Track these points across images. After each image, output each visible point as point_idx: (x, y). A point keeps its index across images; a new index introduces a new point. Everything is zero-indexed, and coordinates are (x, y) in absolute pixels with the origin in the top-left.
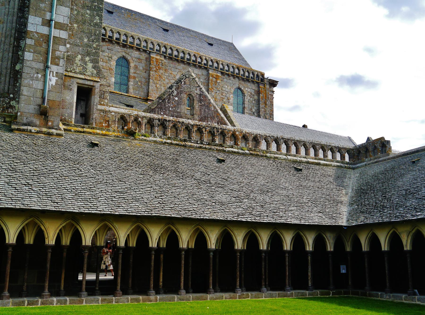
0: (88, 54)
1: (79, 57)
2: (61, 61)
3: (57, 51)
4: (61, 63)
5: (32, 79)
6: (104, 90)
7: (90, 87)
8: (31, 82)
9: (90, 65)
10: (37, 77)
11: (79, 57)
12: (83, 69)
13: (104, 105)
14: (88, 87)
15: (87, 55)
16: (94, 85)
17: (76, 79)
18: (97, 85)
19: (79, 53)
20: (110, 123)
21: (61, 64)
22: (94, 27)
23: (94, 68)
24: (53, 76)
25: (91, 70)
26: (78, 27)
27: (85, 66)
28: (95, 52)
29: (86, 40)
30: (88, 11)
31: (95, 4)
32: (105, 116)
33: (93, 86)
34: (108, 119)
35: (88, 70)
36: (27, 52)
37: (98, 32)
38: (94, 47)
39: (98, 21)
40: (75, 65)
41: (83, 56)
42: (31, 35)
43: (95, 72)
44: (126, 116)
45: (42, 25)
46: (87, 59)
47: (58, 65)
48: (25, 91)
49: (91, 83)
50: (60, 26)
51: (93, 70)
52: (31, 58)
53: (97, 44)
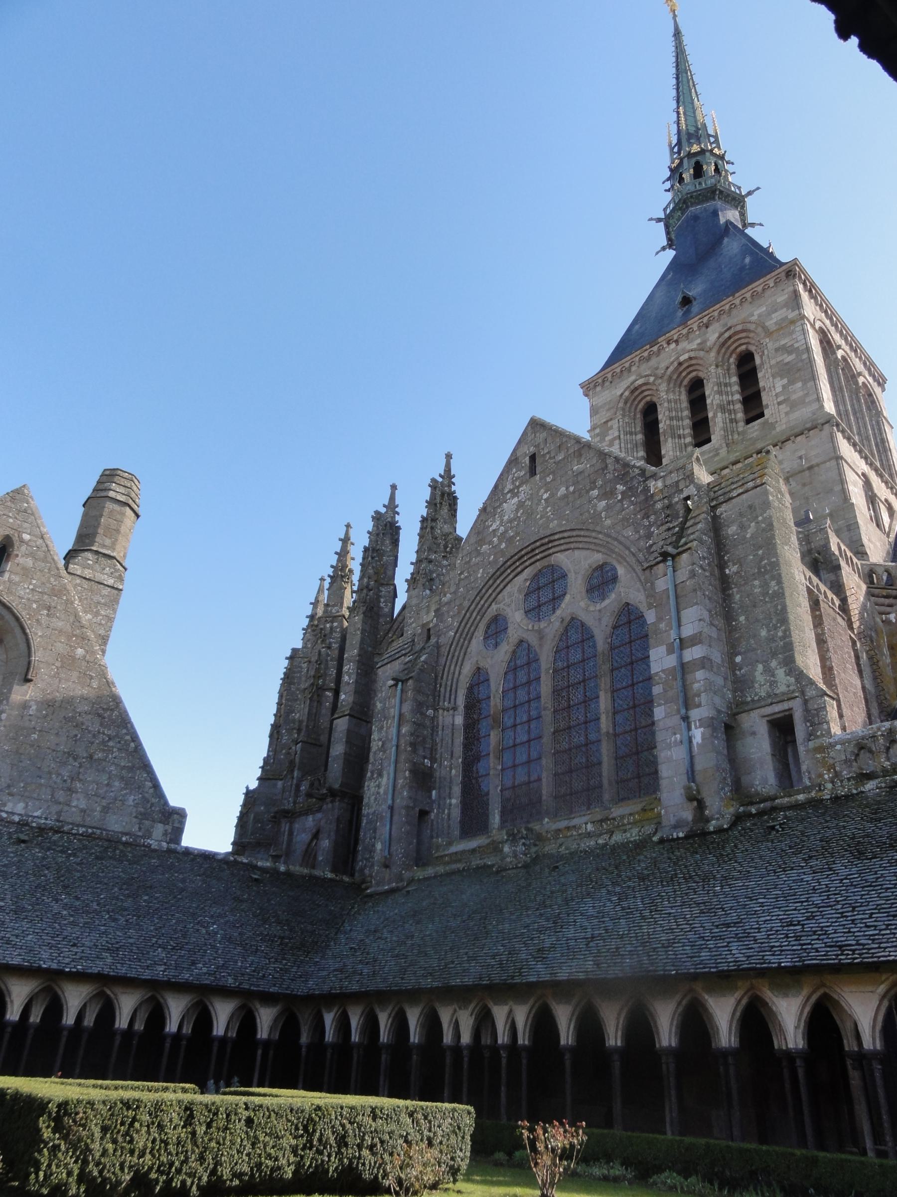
0: (774, 654)
1: (760, 667)
2: (703, 695)
3: (694, 683)
4: (702, 700)
5: (669, 746)
6: (816, 706)
7: (787, 713)
8: (669, 753)
9: (780, 673)
10: (676, 740)
11: (760, 667)
12: (771, 685)
13: (822, 735)
14: (785, 715)
15: (773, 657)
16: (791, 706)
17: (758, 711)
18: (796, 705)
19: (757, 661)
20: (838, 769)
21: (703, 703)
22: (771, 602)
23: (789, 675)
24: (696, 728)
25: (785, 682)
26: (747, 619)
27: (772, 679)
28: (784, 643)
29: (764, 633)
30: (756, 583)
31: (763, 563)
32: (824, 758)
33: (791, 709)
34: (831, 761)
35: (779, 684)
36: (658, 706)
37: (779, 607)
38: (780, 638)
39: (776, 588)
40: (756, 685)
41: (766, 663)
42: (657, 678)
43: (793, 680)
44: (866, 741)
45: (667, 655)
46: (774, 664)
47: (699, 706)
48: (665, 771)
49: (785, 706)
50: (695, 640)
51: (788, 678)
52: (663, 715)
53: (783, 628)
